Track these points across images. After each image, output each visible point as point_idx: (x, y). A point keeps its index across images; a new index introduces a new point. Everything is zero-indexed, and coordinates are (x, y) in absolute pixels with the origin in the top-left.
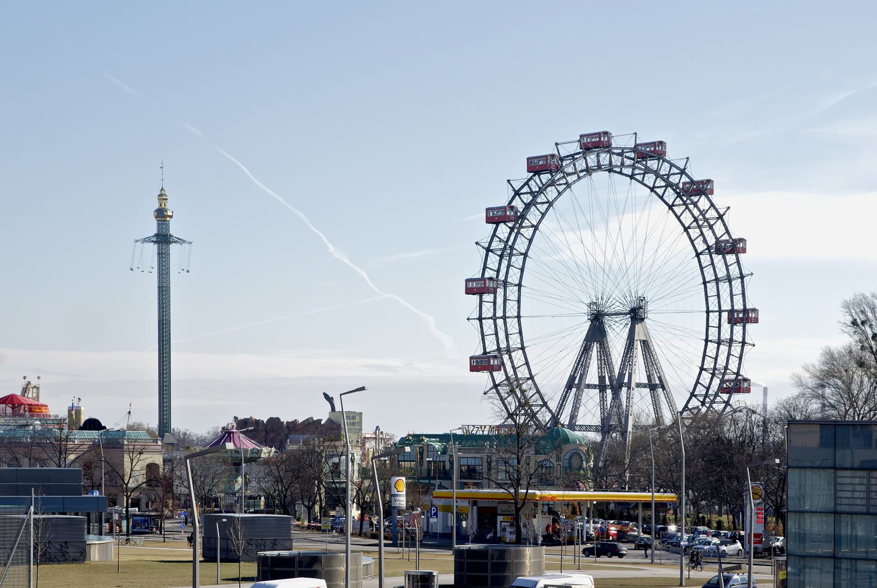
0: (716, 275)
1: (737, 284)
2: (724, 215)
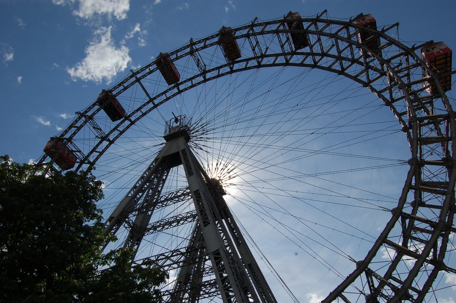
0: (148, 103)
1: (139, 76)
2: (80, 113)
